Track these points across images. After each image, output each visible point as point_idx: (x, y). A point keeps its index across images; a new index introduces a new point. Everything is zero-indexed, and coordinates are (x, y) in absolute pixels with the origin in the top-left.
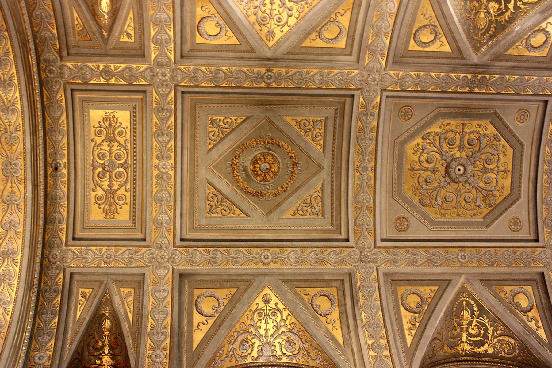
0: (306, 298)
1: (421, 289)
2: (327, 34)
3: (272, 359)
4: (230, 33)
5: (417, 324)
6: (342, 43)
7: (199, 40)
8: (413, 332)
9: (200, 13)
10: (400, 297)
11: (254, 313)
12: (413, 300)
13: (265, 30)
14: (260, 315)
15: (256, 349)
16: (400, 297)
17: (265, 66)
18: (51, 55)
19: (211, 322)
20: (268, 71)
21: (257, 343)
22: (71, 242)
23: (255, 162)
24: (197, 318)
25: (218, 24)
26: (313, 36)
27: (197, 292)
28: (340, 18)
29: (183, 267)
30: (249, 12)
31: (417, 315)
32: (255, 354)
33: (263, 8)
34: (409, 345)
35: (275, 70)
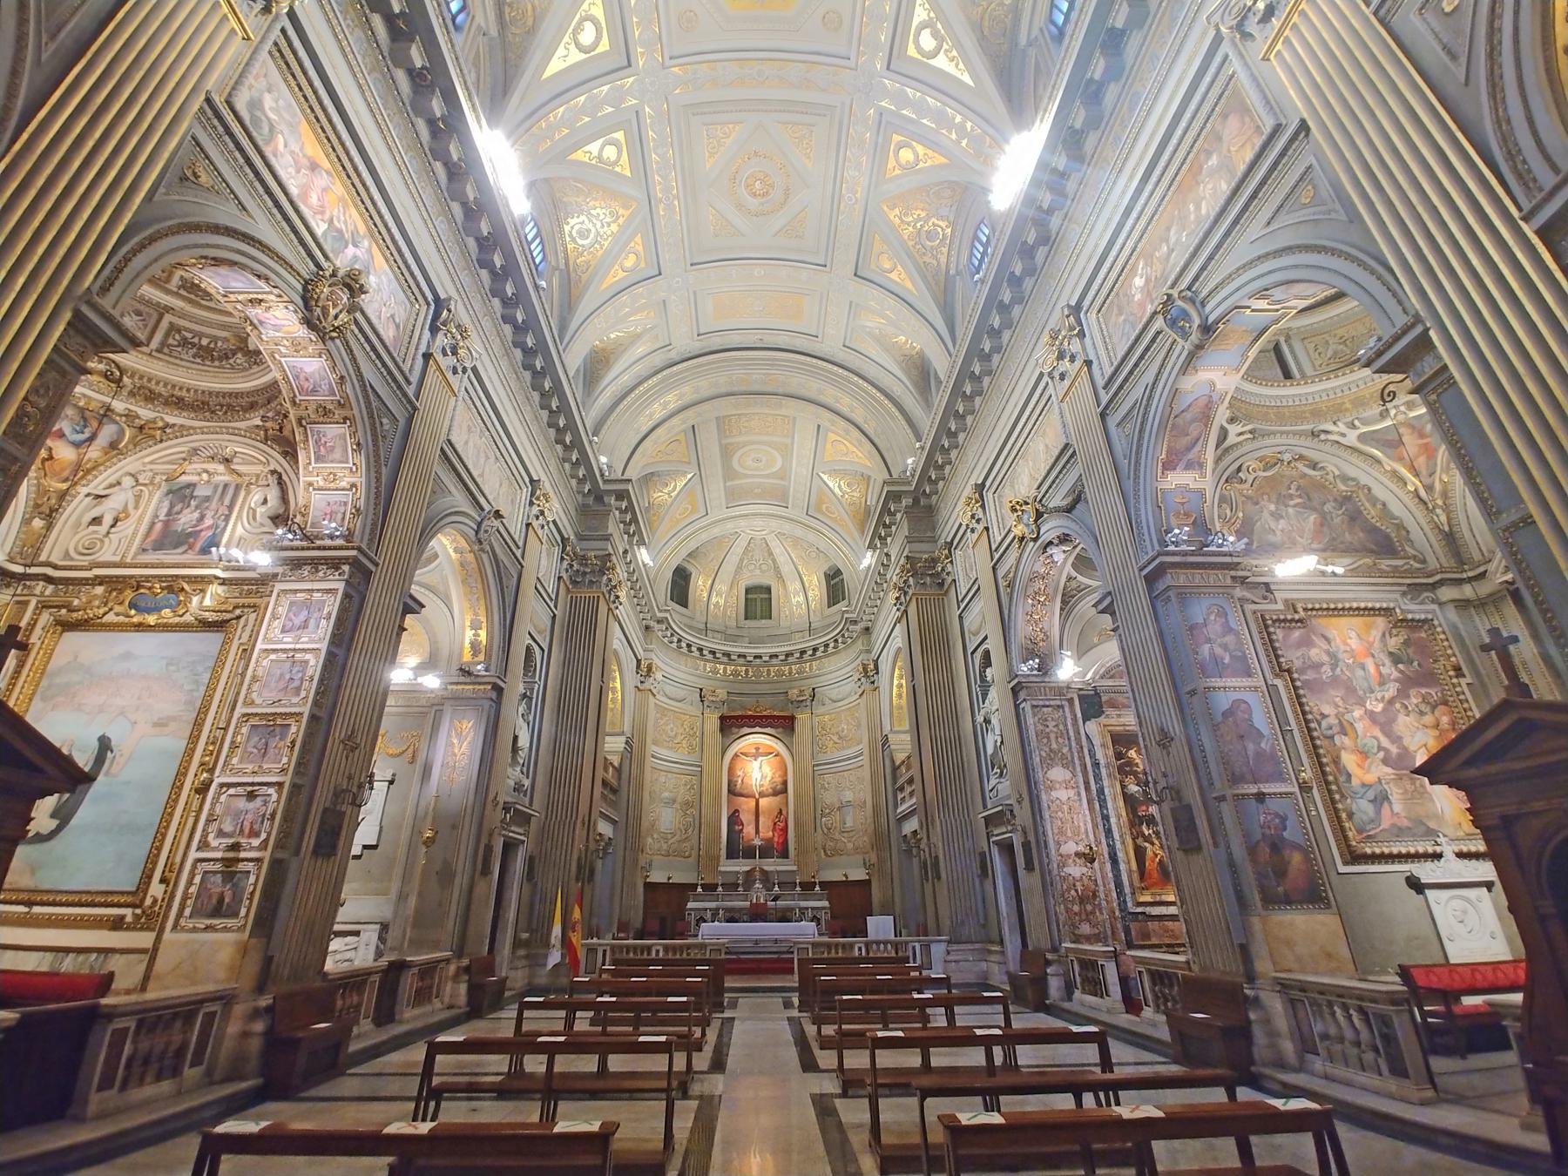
0: (897, 172)
1: (916, 21)
2: (613, 157)
3: (954, 208)
4: (632, 244)
5: (954, 53)
6: (619, 135)
7: (643, 265)
8: (961, 66)
9: (621, 274)
10: (920, 57)
11: (902, 221)
12: (927, 41)
13: (621, 211)
14: (906, 215)
15: (941, 223)
16: (920, 57)
17: (657, 207)
18: (674, 355)
19: (899, 267)
20: (661, 201)
21: (934, 220)
22: (820, 339)
23: (755, 195)
24: (894, 276)
25: (627, 257)
26: (618, 169)
27: (873, 266)
28: (595, 153)
29: (850, 269)
30: (609, 233)
31: (945, 46)
32: (943, 224)
33: (602, 217)
34: (972, 84)
35: (660, 195)
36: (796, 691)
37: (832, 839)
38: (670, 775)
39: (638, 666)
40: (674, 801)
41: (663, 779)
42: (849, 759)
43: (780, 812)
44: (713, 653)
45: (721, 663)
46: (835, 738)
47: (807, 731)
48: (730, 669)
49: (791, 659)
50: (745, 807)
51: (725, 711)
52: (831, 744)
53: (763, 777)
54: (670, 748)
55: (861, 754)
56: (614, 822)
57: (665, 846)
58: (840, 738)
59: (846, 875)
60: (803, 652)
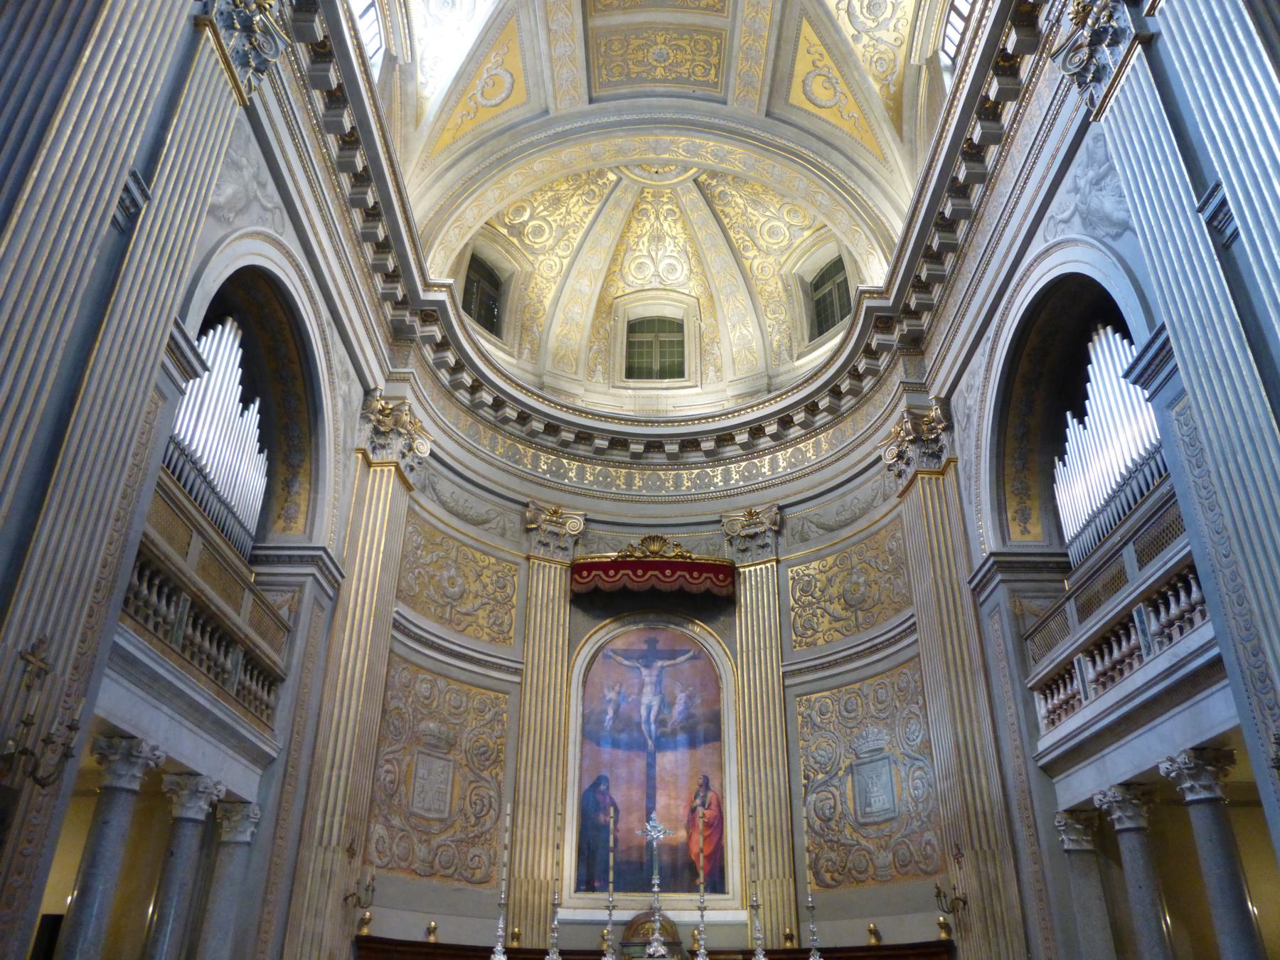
36: (740, 516)
37: (835, 844)
38: (441, 683)
39: (366, 405)
40: (451, 745)
41: (424, 688)
42: (875, 649)
43: (706, 785)
44: (553, 428)
45: (574, 457)
46: (836, 608)
47: (768, 599)
48: (592, 472)
49: (730, 451)
50: (622, 772)
51: (581, 554)
52: (825, 623)
53: (667, 704)
54: (440, 619)
55: (912, 629)
56: (262, 760)
57: (421, 851)
58: (848, 606)
59: (874, 933)
60: (756, 430)
